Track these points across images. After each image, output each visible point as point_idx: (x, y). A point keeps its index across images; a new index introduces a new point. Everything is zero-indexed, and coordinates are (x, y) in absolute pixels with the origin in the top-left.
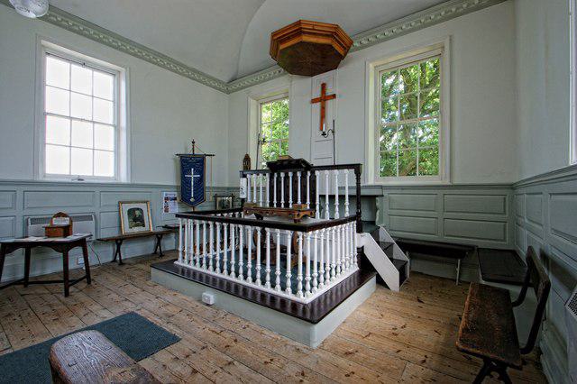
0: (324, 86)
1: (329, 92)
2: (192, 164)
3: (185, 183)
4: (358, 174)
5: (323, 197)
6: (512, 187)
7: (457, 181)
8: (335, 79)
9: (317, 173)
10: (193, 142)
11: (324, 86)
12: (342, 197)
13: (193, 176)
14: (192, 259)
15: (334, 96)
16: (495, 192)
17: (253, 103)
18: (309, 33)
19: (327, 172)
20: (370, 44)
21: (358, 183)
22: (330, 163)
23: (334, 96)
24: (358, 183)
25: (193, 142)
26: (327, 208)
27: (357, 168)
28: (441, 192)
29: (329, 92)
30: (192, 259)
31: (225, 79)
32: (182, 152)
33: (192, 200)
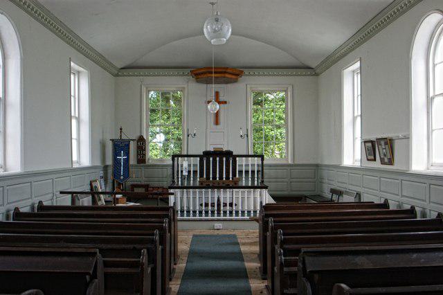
0: (217, 94)
1: (221, 99)
2: (120, 146)
3: (116, 162)
4: (263, 160)
5: (241, 172)
6: (317, 166)
7: (296, 163)
8: (226, 91)
9: (237, 159)
10: (121, 129)
11: (217, 94)
12: (253, 172)
13: (122, 158)
14: (210, 208)
15: (225, 102)
16: (312, 168)
17: (144, 89)
18: (230, 74)
19: (244, 158)
20: (254, 75)
21: (262, 163)
22: (245, 153)
23: (225, 102)
24: (262, 163)
25: (121, 129)
26: (192, 179)
27: (262, 157)
28: (289, 168)
29: (221, 99)
30: (210, 208)
31: (119, 65)
32: (118, 137)
33: (122, 177)
